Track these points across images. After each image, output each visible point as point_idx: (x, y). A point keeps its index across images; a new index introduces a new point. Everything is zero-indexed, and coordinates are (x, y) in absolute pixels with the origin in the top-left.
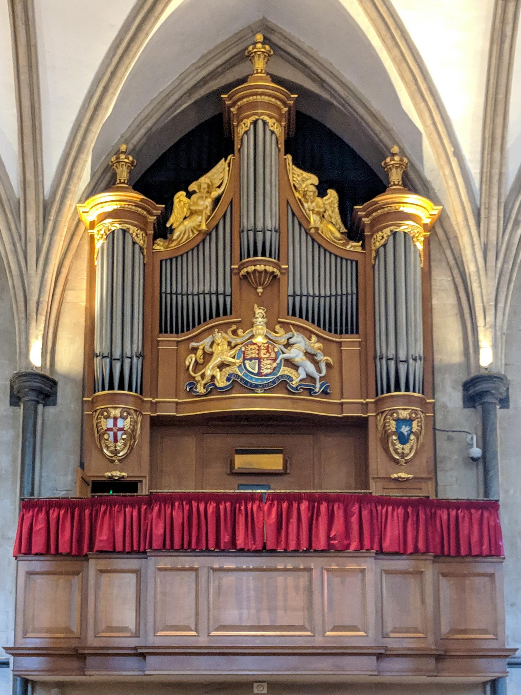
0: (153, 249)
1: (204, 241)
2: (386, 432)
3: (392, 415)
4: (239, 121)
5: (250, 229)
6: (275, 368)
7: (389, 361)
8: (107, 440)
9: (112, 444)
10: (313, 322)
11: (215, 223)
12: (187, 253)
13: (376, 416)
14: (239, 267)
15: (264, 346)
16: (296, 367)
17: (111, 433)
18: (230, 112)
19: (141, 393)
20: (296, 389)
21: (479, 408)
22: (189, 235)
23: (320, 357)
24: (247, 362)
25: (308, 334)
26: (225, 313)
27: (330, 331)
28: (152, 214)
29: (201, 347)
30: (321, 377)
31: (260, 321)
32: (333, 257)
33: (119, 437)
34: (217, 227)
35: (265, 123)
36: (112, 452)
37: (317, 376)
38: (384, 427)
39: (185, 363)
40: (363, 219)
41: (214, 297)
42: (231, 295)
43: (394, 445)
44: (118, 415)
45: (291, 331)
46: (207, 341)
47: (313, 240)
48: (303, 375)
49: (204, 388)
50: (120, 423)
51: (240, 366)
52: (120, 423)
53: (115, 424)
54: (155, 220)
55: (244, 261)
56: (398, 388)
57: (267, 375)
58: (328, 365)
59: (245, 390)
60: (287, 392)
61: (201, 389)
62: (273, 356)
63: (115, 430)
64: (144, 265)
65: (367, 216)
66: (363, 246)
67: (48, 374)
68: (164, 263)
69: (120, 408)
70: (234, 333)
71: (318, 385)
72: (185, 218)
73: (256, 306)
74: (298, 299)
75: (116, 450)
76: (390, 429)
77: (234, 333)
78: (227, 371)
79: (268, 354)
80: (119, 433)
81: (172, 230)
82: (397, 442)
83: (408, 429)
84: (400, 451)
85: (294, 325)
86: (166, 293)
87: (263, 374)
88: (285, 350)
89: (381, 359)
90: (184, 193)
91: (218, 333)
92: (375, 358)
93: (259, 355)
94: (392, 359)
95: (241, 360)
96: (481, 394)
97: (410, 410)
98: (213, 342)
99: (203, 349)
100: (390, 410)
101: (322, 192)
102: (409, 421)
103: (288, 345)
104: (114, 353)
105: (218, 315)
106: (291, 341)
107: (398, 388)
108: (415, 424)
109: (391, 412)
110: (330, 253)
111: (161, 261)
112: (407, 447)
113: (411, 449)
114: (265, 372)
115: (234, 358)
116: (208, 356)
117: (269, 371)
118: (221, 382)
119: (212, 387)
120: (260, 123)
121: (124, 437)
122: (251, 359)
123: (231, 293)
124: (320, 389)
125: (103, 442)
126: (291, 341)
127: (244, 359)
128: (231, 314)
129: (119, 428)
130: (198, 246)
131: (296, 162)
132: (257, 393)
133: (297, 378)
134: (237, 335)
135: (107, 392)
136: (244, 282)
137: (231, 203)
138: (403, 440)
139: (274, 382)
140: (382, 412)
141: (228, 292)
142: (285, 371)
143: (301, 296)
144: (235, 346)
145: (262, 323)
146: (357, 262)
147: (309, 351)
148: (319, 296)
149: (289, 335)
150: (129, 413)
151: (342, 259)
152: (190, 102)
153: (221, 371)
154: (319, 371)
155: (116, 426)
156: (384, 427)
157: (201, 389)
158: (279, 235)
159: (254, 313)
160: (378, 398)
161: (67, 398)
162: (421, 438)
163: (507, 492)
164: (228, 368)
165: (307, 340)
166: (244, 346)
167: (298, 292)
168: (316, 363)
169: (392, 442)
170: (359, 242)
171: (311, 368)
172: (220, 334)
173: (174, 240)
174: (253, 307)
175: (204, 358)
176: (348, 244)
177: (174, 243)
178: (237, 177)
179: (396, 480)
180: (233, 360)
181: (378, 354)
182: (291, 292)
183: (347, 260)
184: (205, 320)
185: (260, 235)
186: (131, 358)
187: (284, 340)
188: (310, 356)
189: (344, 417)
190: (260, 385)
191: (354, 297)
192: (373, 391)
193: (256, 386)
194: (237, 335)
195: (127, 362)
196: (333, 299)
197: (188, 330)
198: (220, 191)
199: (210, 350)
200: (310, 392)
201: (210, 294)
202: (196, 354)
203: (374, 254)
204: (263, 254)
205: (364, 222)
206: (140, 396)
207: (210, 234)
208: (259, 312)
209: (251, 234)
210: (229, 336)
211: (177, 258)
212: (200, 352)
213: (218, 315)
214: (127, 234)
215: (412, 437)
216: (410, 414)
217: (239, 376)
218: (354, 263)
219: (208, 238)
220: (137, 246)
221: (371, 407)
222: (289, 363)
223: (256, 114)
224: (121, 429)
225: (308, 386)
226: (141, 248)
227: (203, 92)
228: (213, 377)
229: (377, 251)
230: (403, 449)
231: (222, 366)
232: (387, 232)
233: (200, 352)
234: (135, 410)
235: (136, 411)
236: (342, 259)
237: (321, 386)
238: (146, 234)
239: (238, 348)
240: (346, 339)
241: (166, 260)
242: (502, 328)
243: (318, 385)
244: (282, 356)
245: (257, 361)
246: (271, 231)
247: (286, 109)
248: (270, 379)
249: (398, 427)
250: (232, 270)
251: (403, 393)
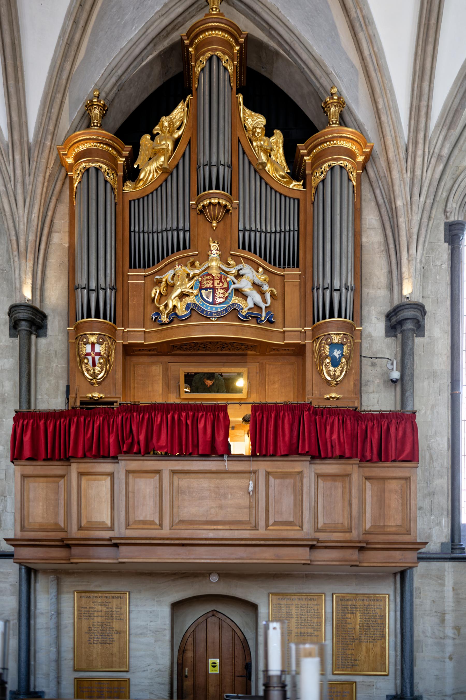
0: (124, 190)
1: (166, 180)
2: (321, 356)
3: (326, 340)
4: (196, 60)
5: (205, 164)
6: (227, 297)
7: (325, 290)
8: (87, 364)
9: (91, 368)
10: (260, 256)
11: (176, 163)
12: (152, 193)
13: (313, 342)
14: (196, 203)
15: (218, 276)
16: (245, 297)
17: (90, 358)
18: (188, 52)
19: (115, 323)
20: (245, 317)
22: (153, 175)
23: (266, 288)
24: (203, 291)
25: (256, 266)
26: (185, 248)
27: (275, 265)
28: (121, 156)
29: (164, 280)
30: (266, 307)
31: (214, 253)
32: (278, 196)
33: (97, 361)
34: (177, 167)
35: (219, 59)
36: (91, 375)
37: (263, 306)
38: (320, 351)
39: (151, 295)
40: (305, 158)
41: (175, 233)
42: (189, 231)
43: (327, 367)
44: (95, 341)
45: (242, 263)
46: (170, 274)
47: (261, 178)
48: (251, 305)
49: (167, 317)
50: (98, 348)
51: (197, 295)
54: (124, 162)
55: (200, 195)
56: (332, 316)
57: (220, 303)
58: (272, 295)
59: (201, 318)
60: (238, 319)
61: (164, 318)
62: (225, 285)
63: (93, 355)
64: (116, 204)
65: (308, 154)
66: (304, 185)
67: (37, 305)
68: (132, 202)
69: (97, 334)
70: (193, 265)
71: (264, 314)
72: (150, 159)
73: (211, 239)
74: (247, 234)
75: (94, 373)
76: (324, 353)
77: (193, 265)
79: (221, 284)
80: (97, 358)
81: (138, 171)
82: (330, 365)
83: (339, 352)
84: (332, 372)
85: (243, 257)
86: (135, 232)
87: (217, 303)
88: (235, 280)
89: (318, 289)
90: (148, 137)
91: (178, 265)
92: (313, 289)
93: (214, 286)
94: (327, 288)
95: (198, 290)
96: (401, 323)
97: (342, 335)
98: (174, 275)
99: (166, 281)
100: (325, 335)
101: (269, 133)
102: (340, 346)
103: (238, 276)
104: (90, 285)
105: (178, 249)
106: (241, 272)
108: (345, 347)
109: (326, 337)
110: (276, 192)
111: (130, 201)
112: (338, 369)
113: (342, 371)
114: (219, 300)
115: (192, 288)
116: (170, 287)
117: (222, 300)
118: (182, 311)
119: (174, 316)
120: (215, 59)
121: (101, 361)
122: (206, 289)
123: (190, 228)
124: (265, 318)
125: (83, 366)
126: (241, 272)
127: (201, 289)
128: (189, 248)
129: (96, 353)
130: (161, 186)
131: (247, 104)
132: (212, 321)
133: (246, 306)
134: (195, 267)
135: (86, 320)
136: (201, 217)
137: (189, 143)
138: (335, 363)
139: (226, 310)
140: (318, 338)
141: (187, 228)
142: (236, 300)
143: (250, 231)
144: (193, 277)
145: (216, 255)
146: (299, 200)
147: (256, 282)
148: (266, 232)
149: (240, 266)
150: (103, 340)
151: (285, 197)
152: (155, 54)
153: (181, 301)
154: (265, 301)
155: (94, 351)
156: (320, 351)
157: (164, 318)
158: (231, 171)
159: (210, 246)
160: (315, 325)
161: (56, 326)
164: (187, 298)
165: (254, 271)
166: (201, 277)
167: (248, 228)
168: (262, 293)
169: (326, 364)
170: (300, 181)
171: (258, 298)
172: (180, 266)
173: (141, 180)
174: (209, 241)
175: (167, 290)
176: (292, 183)
177: (141, 183)
178: (193, 115)
179: (328, 399)
180: (191, 291)
181: (316, 285)
182: (241, 228)
183: (290, 198)
184: (168, 255)
185: (214, 170)
186: (105, 289)
187: (234, 271)
188: (257, 286)
189: (285, 343)
190: (215, 313)
191: (296, 233)
192: (310, 318)
193: (211, 314)
194: (195, 267)
195: (101, 293)
196: (278, 235)
197: (154, 264)
198: (180, 132)
199: (172, 282)
200: (258, 320)
201: (172, 230)
202: (160, 287)
203: (314, 191)
204: (217, 188)
205: (305, 160)
206: (114, 325)
207: (171, 174)
208: (214, 246)
209: (207, 168)
210: (188, 270)
211: (143, 198)
212: (163, 284)
213: (178, 249)
214: (100, 173)
215: (343, 360)
216: (342, 339)
217: (197, 305)
218: (296, 202)
219: (170, 177)
220: (108, 185)
221: (309, 334)
223: (211, 50)
224: (98, 354)
225: (254, 315)
226: (112, 189)
227: (166, 44)
228: (175, 307)
229: (317, 188)
230: (335, 371)
231: (183, 296)
233: (163, 284)
234: (110, 338)
235: (110, 338)
236: (285, 197)
237: (267, 314)
238: (117, 175)
239: (196, 278)
240: (288, 272)
241: (134, 200)
242: (421, 261)
243: (264, 314)
244: (233, 286)
245: (212, 290)
246: (224, 165)
247: (238, 48)
248: (223, 307)
249: (331, 351)
250: (190, 205)
251: (336, 319)
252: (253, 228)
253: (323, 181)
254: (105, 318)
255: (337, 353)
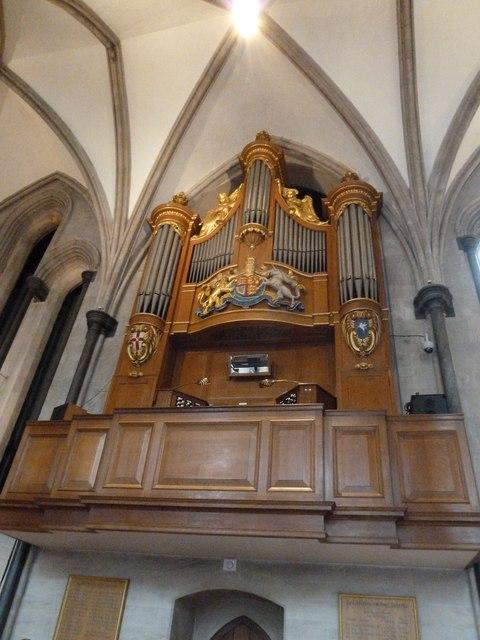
21: (429, 316)
37: (293, 297)
50: (142, 335)
52: (142, 335)
53: (138, 336)
56: (355, 296)
58: (301, 291)
78: (225, 296)
103: (270, 277)
107: (355, 296)
116: (212, 290)
133: (274, 297)
162: (378, 334)
163: (462, 380)
168: (293, 290)
186: (159, 295)
193: (243, 303)
222: (269, 287)
225: (283, 305)
228: (214, 303)
232: (343, 206)
252: (286, 248)
253: (342, 215)
254: (155, 312)
255: (362, 326)
